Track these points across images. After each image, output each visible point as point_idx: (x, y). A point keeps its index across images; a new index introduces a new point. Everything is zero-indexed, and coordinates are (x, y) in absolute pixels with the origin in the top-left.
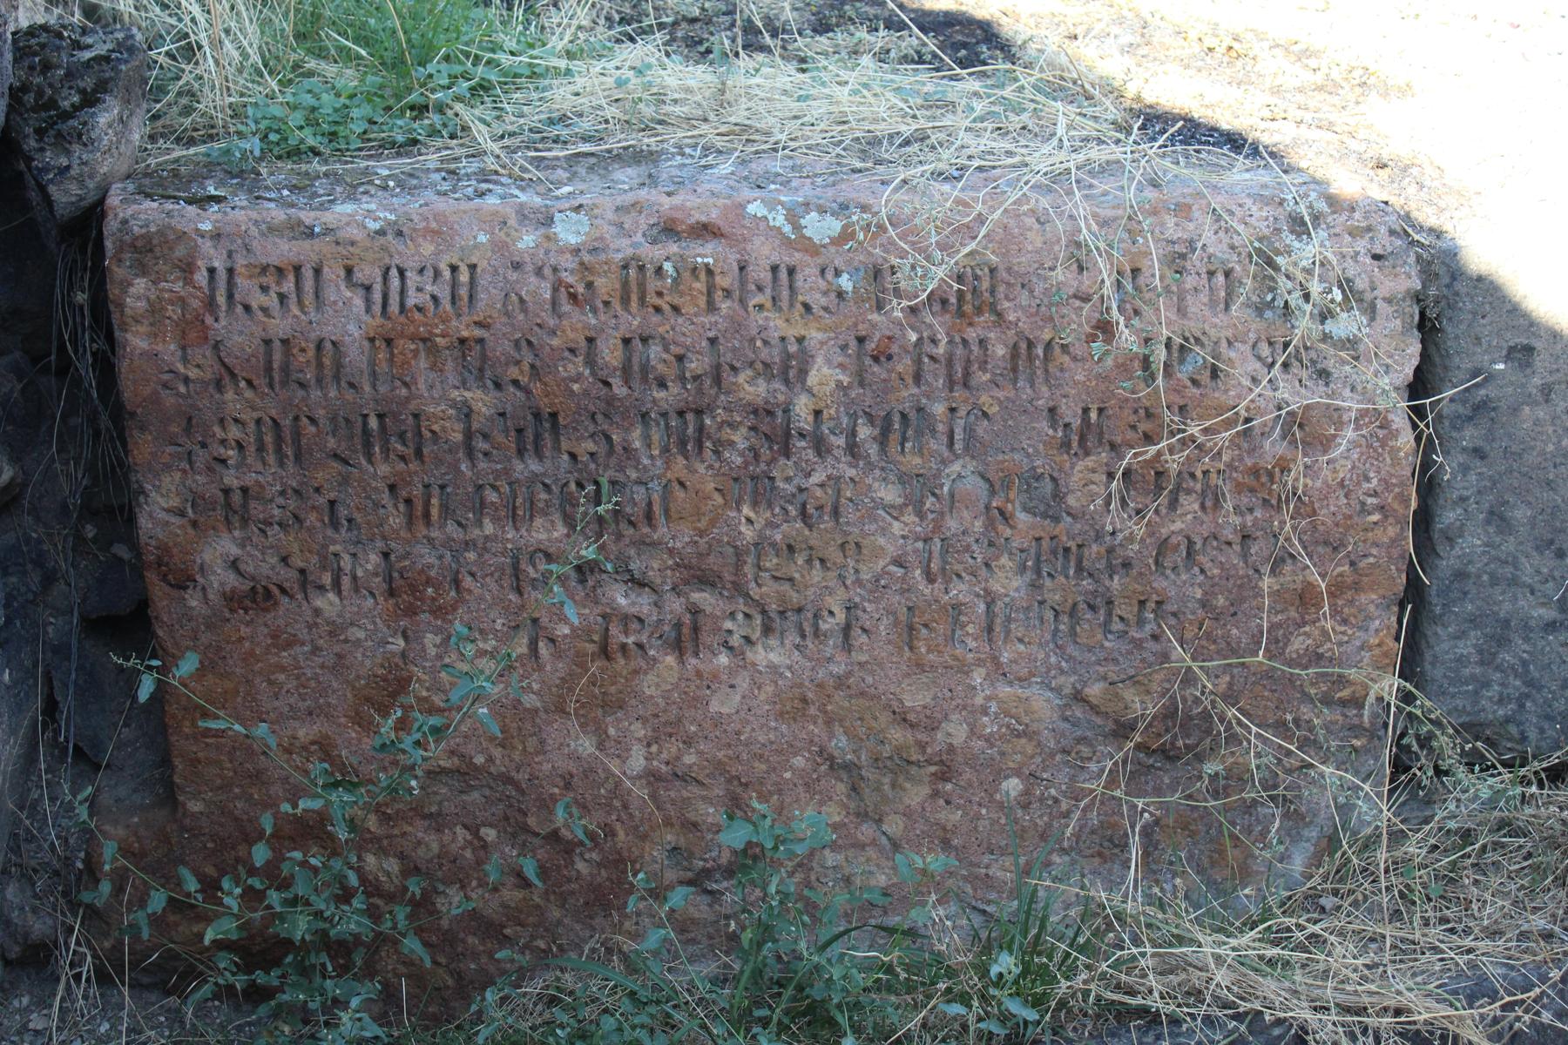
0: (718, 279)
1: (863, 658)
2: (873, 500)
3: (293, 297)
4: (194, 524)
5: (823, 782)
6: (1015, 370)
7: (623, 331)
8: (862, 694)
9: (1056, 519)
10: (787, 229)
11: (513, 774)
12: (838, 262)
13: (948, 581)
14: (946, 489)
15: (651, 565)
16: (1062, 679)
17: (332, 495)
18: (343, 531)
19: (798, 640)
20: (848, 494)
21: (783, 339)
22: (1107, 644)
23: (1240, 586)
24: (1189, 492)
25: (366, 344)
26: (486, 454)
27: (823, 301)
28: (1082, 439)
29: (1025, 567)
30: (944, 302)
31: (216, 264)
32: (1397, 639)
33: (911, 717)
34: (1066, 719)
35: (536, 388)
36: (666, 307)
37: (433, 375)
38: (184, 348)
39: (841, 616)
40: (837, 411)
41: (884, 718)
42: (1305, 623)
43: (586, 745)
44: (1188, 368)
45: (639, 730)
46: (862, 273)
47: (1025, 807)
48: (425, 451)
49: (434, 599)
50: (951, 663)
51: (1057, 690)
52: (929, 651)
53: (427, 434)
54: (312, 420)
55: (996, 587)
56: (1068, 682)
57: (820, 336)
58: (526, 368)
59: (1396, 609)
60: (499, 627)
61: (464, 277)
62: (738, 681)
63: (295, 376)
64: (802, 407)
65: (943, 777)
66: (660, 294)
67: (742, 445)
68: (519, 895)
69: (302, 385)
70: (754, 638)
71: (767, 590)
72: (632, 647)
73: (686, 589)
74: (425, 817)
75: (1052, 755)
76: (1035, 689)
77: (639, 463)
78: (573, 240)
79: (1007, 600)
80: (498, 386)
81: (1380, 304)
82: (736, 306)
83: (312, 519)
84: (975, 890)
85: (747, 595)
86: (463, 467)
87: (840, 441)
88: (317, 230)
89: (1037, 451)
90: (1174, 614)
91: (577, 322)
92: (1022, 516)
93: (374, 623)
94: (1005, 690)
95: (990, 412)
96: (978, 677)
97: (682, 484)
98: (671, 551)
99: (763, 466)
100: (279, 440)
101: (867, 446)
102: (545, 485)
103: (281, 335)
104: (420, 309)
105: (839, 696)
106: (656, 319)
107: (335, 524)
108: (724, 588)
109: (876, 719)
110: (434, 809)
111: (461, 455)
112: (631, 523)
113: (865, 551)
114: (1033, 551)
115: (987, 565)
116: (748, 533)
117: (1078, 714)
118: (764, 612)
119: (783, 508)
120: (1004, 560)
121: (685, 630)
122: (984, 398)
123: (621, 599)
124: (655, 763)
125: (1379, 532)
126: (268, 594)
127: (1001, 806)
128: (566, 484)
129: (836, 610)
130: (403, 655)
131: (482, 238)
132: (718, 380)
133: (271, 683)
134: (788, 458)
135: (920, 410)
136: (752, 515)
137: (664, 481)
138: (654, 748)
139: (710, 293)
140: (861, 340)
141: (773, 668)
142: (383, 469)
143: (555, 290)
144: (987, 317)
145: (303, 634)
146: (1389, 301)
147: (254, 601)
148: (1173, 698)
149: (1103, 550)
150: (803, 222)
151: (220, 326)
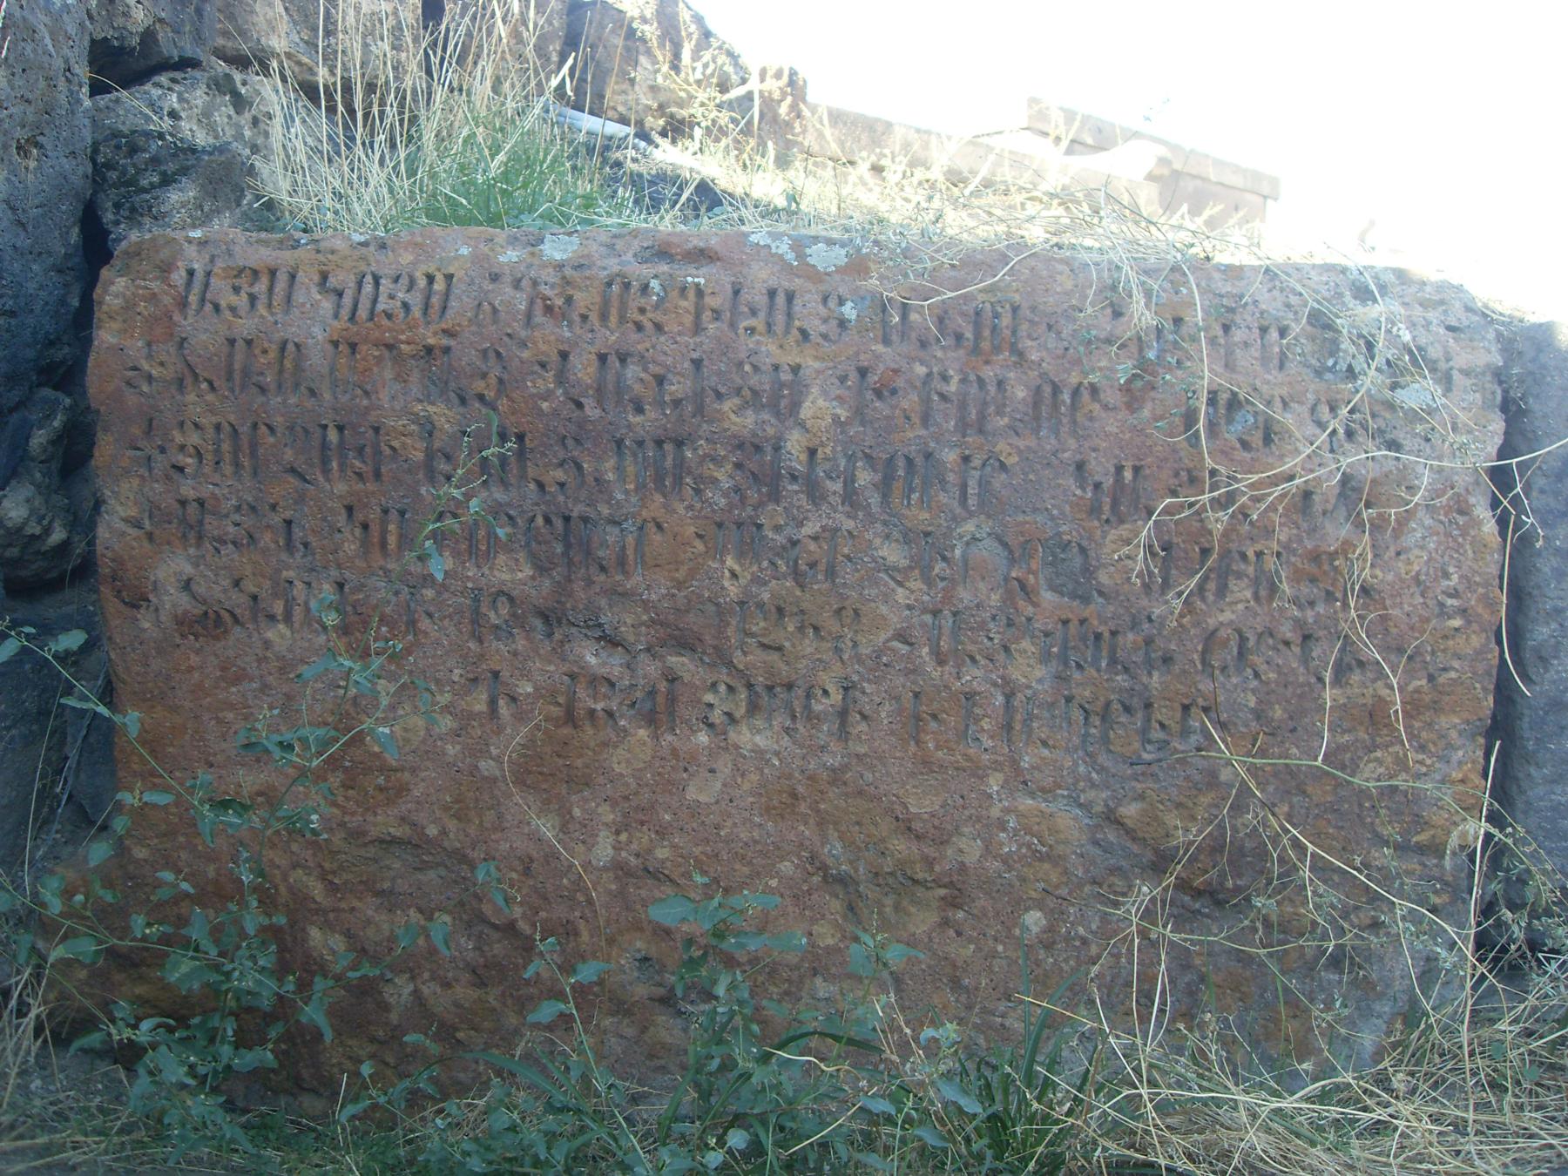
0: (708, 300)
1: (862, 750)
2: (874, 560)
3: (263, 299)
4: (150, 536)
5: (815, 896)
6: (1037, 418)
7: (600, 346)
8: (860, 793)
9: (1086, 600)
10: (790, 256)
11: (468, 851)
13: (959, 666)
14: (958, 552)
15: (623, 620)
16: (1091, 794)
17: (288, 514)
18: (298, 556)
19: (788, 723)
20: (846, 551)
21: (776, 368)
23: (1301, 696)
24: (1239, 575)
25: (330, 347)
27: (823, 328)
28: (1115, 504)
29: (1049, 653)
30: (959, 337)
31: (196, 266)
32: (1485, 777)
33: (917, 825)
34: (1096, 843)
36: (648, 325)
37: (398, 386)
38: (149, 344)
39: (836, 697)
40: (834, 450)
43: (547, 828)
44: (1237, 427)
45: (607, 814)
46: (867, 303)
47: (1049, 946)
48: (383, 470)
50: (965, 764)
51: (1086, 807)
52: (938, 747)
53: (388, 451)
54: (271, 428)
55: (1015, 675)
56: (1099, 798)
57: (817, 365)
58: (493, 381)
59: (1482, 740)
60: (456, 679)
62: (719, 765)
63: (255, 379)
64: (795, 443)
65: (953, 903)
66: (642, 311)
68: (474, 994)
69: (263, 390)
70: (737, 715)
71: (751, 659)
72: (601, 714)
73: (663, 651)
74: (379, 894)
75: (1080, 886)
76: (1061, 804)
77: (611, 497)
78: (558, 256)
79: (1029, 692)
80: (463, 401)
81: (1456, 375)
82: (725, 327)
83: (266, 539)
84: (987, 1040)
86: (423, 491)
87: (838, 486)
89: (1062, 513)
91: (549, 334)
92: (1047, 596)
96: (994, 784)
97: (659, 527)
98: (645, 603)
100: (236, 451)
101: (867, 494)
102: (511, 518)
104: (389, 316)
105: (833, 792)
106: (635, 336)
108: (704, 653)
109: (876, 825)
110: (386, 885)
111: (421, 476)
112: (603, 569)
114: (1059, 634)
115: (1006, 649)
116: (733, 590)
117: (1112, 837)
118: (750, 686)
119: (773, 563)
120: (1025, 644)
121: (660, 699)
122: (1001, 446)
123: (591, 657)
124: (624, 854)
125: (1461, 639)
126: (218, 621)
128: (532, 519)
129: (831, 689)
132: (700, 410)
133: (220, 721)
134: (777, 502)
135: (928, 456)
136: (737, 567)
137: (639, 521)
138: (624, 837)
139: (698, 316)
140: (863, 372)
141: (759, 753)
142: (340, 488)
143: (532, 303)
146: (1466, 373)
147: (205, 628)
148: (1221, 826)
149: (1140, 639)
150: (808, 251)
151: (186, 324)
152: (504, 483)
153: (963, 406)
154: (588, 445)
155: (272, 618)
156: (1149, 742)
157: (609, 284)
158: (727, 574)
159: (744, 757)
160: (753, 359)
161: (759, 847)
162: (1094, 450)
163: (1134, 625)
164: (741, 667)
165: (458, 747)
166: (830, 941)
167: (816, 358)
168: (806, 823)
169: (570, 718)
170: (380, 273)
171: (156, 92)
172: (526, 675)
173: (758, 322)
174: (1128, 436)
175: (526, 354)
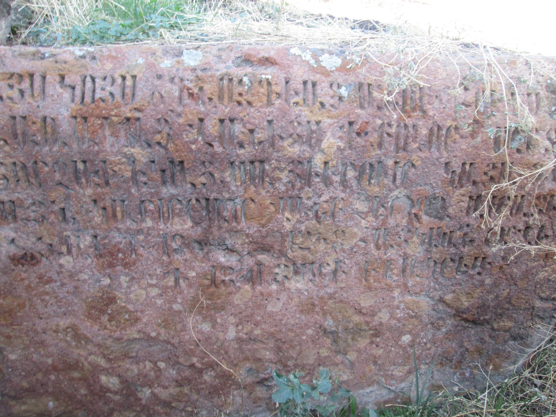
0: (274, 87)
1: (343, 285)
2: (353, 210)
5: (321, 339)
6: (430, 142)
9: (441, 219)
10: (312, 62)
11: (171, 340)
12: (340, 80)
13: (386, 249)
14: (390, 204)
15: (237, 242)
17: (62, 205)
18: (71, 224)
19: (311, 277)
20: (340, 206)
22: (457, 277)
26: (145, 184)
27: (332, 101)
28: (460, 178)
29: (424, 242)
33: (364, 311)
34: (434, 310)
35: (171, 146)
36: (244, 103)
39: (333, 266)
40: (337, 163)
41: (351, 311)
42: (546, 266)
43: (206, 327)
45: (232, 320)
46: (352, 87)
47: (411, 346)
49: (123, 260)
50: (385, 287)
51: (432, 298)
52: (374, 282)
53: (111, 172)
54: (46, 164)
55: (409, 252)
56: (437, 294)
57: (329, 121)
58: (165, 136)
60: (158, 273)
61: (129, 82)
62: (281, 297)
63: (31, 138)
64: (318, 160)
65: (376, 335)
66: (240, 95)
67: (285, 180)
68: (178, 390)
69: (37, 144)
70: (289, 276)
71: (295, 253)
73: (255, 253)
75: (426, 325)
77: (229, 189)
78: (193, 64)
80: (149, 145)
83: (52, 217)
84: (386, 380)
85: (286, 256)
86: (133, 191)
87: (337, 178)
88: (47, 55)
89: (437, 185)
90: (489, 263)
92: (425, 218)
93: (92, 271)
94: (408, 298)
95: (416, 164)
96: (396, 293)
97: (253, 200)
98: (247, 235)
100: (27, 175)
101: (351, 181)
102: (179, 200)
103: (21, 114)
107: (65, 219)
108: (274, 253)
109: (347, 312)
110: (134, 354)
111: (131, 184)
113: (347, 235)
116: (288, 226)
117: (441, 308)
118: (294, 264)
119: (305, 213)
121: (254, 273)
122: (414, 157)
123: (222, 258)
124: (240, 334)
126: (33, 257)
127: (401, 346)
129: (331, 263)
130: (109, 286)
131: (141, 61)
132: (273, 145)
133: (43, 300)
134: (310, 187)
135: (380, 162)
136: (290, 217)
137: (243, 199)
138: (240, 327)
140: (351, 123)
141: (299, 291)
143: (181, 91)
144: (418, 113)
145: (55, 277)
147: (26, 261)
149: (462, 234)
150: (321, 58)
152: (173, 182)
154: (217, 165)
155: (60, 253)
156: (459, 271)
157: (222, 79)
158: (285, 219)
159: (292, 293)
160: (298, 119)
161: (298, 326)
162: (455, 157)
163: (461, 228)
164: (291, 257)
165: (162, 301)
166: (326, 354)
167: (329, 117)
168: (318, 315)
169: (214, 282)
170: (95, 75)
172: (192, 269)
174: (470, 150)
175: (181, 121)
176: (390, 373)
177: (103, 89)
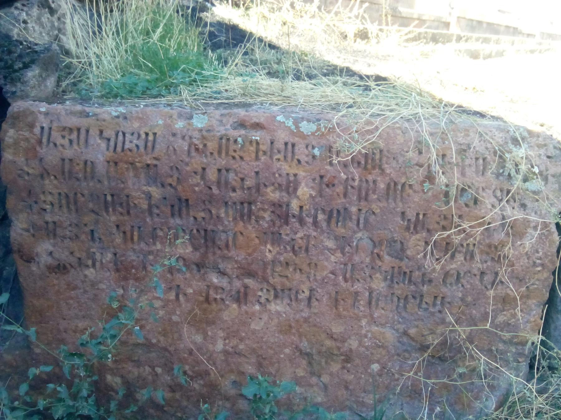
1: (316, 311)
2: (323, 246)
3: (75, 141)
4: (33, 236)
5: (297, 359)
6: (388, 194)
7: (218, 166)
8: (315, 326)
9: (401, 260)
10: (293, 127)
11: (168, 347)
12: (314, 143)
13: (353, 282)
15: (228, 267)
16: (399, 326)
17: (92, 228)
18: (97, 243)
19: (289, 302)
20: (313, 243)
21: (288, 174)
22: (419, 313)
23: (478, 293)
25: (106, 164)
26: (158, 215)
27: (306, 159)
30: (359, 163)
31: (44, 125)
32: (542, 319)
33: (335, 336)
34: (399, 342)
35: (179, 188)
36: (237, 157)
37: (135, 179)
38: (27, 160)
39: (307, 293)
40: (310, 207)
41: (323, 336)
42: (504, 310)
43: (199, 338)
44: (464, 199)
45: (221, 334)
46: (324, 148)
47: (380, 376)
48: (131, 212)
49: (135, 274)
51: (397, 330)
52: (344, 310)
54: (83, 195)
55: (374, 286)
56: (401, 327)
58: (175, 179)
59: (542, 307)
61: (151, 138)
64: (295, 205)
66: (235, 151)
67: (268, 219)
68: (170, 395)
69: (78, 179)
71: (276, 280)
72: (219, 300)
74: (134, 361)
75: (393, 356)
76: (388, 329)
78: (200, 126)
79: (378, 292)
80: (163, 186)
81: (550, 178)
82: (268, 158)
83: (83, 237)
84: (357, 407)
85: (268, 282)
86: (148, 220)
87: (310, 220)
88: (90, 114)
89: (395, 230)
90: (449, 303)
91: (197, 161)
92: (387, 258)
93: (110, 282)
94: (375, 328)
95: (376, 212)
96: (364, 322)
97: (241, 233)
98: (236, 262)
99: (277, 228)
100: (68, 203)
101: (322, 223)
102: (183, 230)
103: (69, 157)
104: (130, 150)
105: (305, 326)
106: (232, 162)
107: (93, 239)
108: (258, 278)
109: (320, 336)
110: (136, 358)
112: (220, 248)
113: (318, 267)
114: (390, 272)
115: (371, 277)
116: (269, 256)
118: (275, 289)
120: (378, 275)
122: (374, 206)
123: (215, 279)
124: (227, 347)
125: (540, 275)
126: (65, 267)
127: (371, 375)
128: (192, 230)
129: (305, 290)
130: (122, 296)
131: (160, 122)
132: (258, 190)
133: (67, 304)
134: (287, 225)
135: (346, 209)
136: (271, 249)
137: (234, 232)
138: (227, 341)
139: (257, 153)
140: (322, 177)
141: (278, 313)
142: (113, 218)
143: (190, 146)
144: (377, 171)
145: (80, 285)
146: (553, 176)
148: (446, 337)
149: (421, 274)
150: (300, 125)
151: (42, 151)
152: (180, 216)
153: (360, 190)
154: (214, 204)
155: (87, 266)
156: (421, 308)
157: (221, 139)
158: (267, 251)
159: (273, 314)
160: (279, 172)
161: (277, 344)
162: (409, 207)
163: (419, 269)
164: (272, 283)
165: (164, 312)
166: (302, 374)
167: (304, 171)
168: (294, 336)
169: (207, 300)
170: (125, 131)
171: (16, 12)
172: (190, 286)
173: (280, 156)
174: (422, 202)
175: (188, 168)
176: (361, 399)
177: (131, 142)
